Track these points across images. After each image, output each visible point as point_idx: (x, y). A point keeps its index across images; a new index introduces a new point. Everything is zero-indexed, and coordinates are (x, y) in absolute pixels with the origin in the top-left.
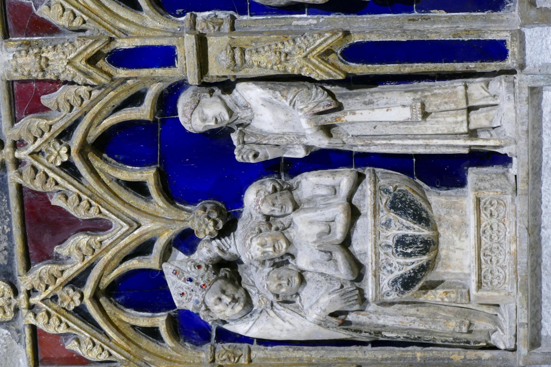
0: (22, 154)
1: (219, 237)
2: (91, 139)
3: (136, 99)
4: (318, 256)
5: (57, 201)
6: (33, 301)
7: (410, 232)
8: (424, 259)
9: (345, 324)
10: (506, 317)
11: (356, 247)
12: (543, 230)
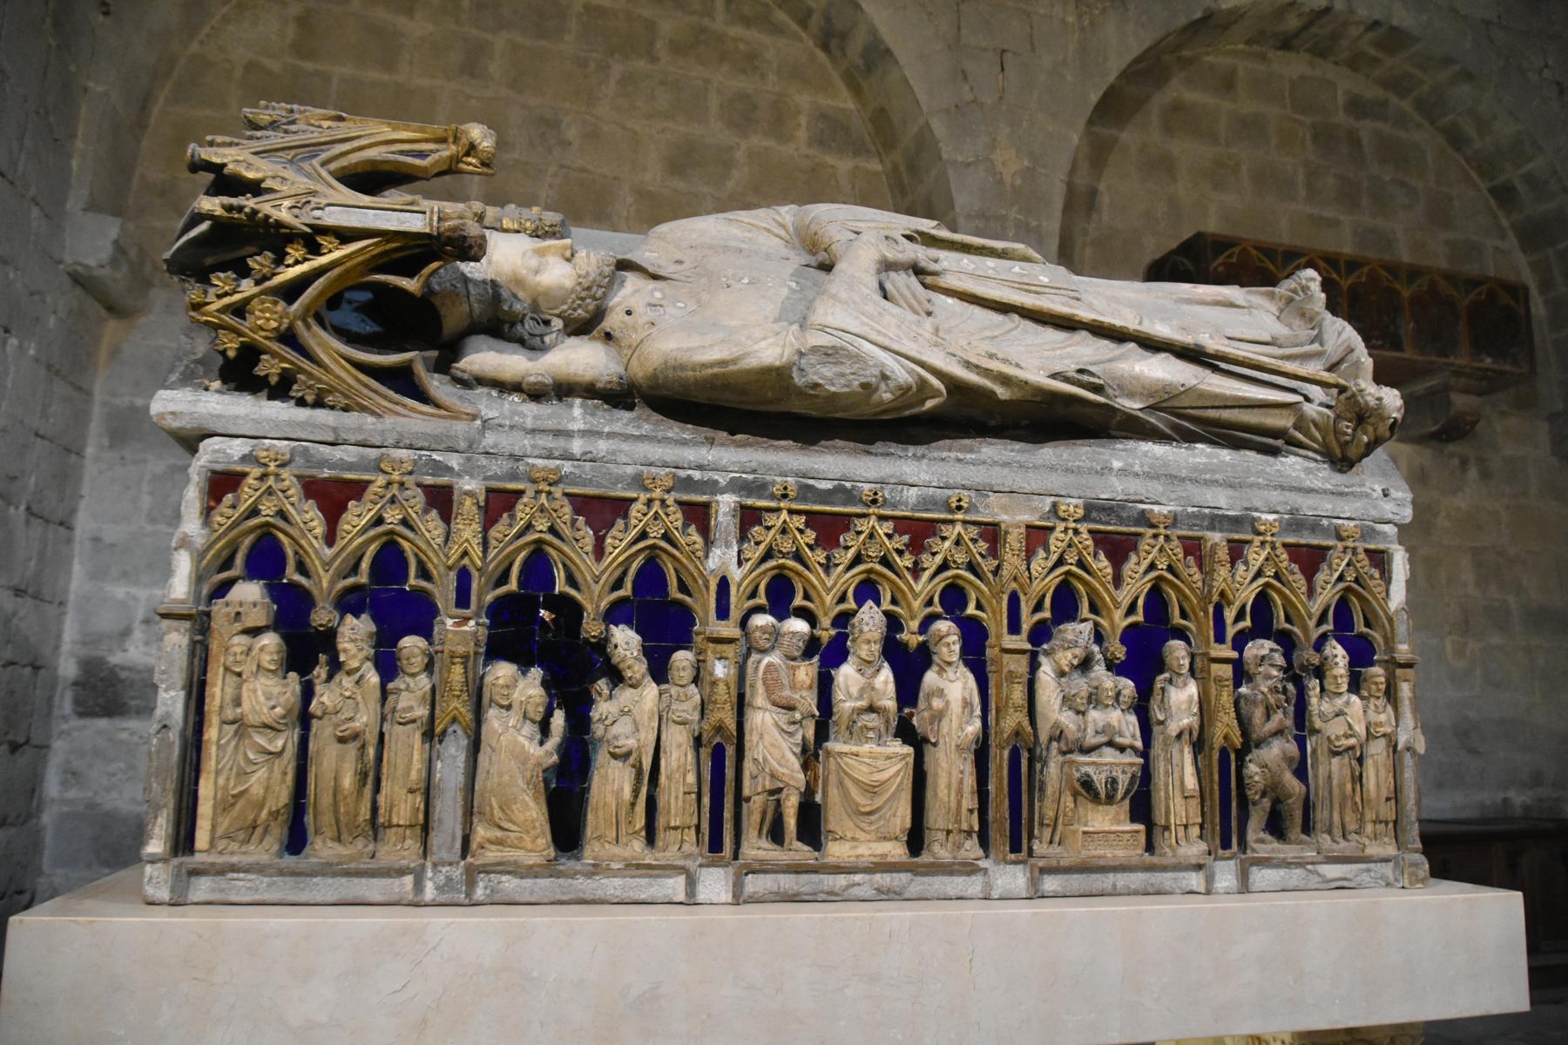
0: (1161, 538)
1: (1106, 659)
3: (1184, 615)
4: (1101, 724)
5: (1133, 558)
9: (1051, 739)
10: (1055, 850)
11: (1108, 750)
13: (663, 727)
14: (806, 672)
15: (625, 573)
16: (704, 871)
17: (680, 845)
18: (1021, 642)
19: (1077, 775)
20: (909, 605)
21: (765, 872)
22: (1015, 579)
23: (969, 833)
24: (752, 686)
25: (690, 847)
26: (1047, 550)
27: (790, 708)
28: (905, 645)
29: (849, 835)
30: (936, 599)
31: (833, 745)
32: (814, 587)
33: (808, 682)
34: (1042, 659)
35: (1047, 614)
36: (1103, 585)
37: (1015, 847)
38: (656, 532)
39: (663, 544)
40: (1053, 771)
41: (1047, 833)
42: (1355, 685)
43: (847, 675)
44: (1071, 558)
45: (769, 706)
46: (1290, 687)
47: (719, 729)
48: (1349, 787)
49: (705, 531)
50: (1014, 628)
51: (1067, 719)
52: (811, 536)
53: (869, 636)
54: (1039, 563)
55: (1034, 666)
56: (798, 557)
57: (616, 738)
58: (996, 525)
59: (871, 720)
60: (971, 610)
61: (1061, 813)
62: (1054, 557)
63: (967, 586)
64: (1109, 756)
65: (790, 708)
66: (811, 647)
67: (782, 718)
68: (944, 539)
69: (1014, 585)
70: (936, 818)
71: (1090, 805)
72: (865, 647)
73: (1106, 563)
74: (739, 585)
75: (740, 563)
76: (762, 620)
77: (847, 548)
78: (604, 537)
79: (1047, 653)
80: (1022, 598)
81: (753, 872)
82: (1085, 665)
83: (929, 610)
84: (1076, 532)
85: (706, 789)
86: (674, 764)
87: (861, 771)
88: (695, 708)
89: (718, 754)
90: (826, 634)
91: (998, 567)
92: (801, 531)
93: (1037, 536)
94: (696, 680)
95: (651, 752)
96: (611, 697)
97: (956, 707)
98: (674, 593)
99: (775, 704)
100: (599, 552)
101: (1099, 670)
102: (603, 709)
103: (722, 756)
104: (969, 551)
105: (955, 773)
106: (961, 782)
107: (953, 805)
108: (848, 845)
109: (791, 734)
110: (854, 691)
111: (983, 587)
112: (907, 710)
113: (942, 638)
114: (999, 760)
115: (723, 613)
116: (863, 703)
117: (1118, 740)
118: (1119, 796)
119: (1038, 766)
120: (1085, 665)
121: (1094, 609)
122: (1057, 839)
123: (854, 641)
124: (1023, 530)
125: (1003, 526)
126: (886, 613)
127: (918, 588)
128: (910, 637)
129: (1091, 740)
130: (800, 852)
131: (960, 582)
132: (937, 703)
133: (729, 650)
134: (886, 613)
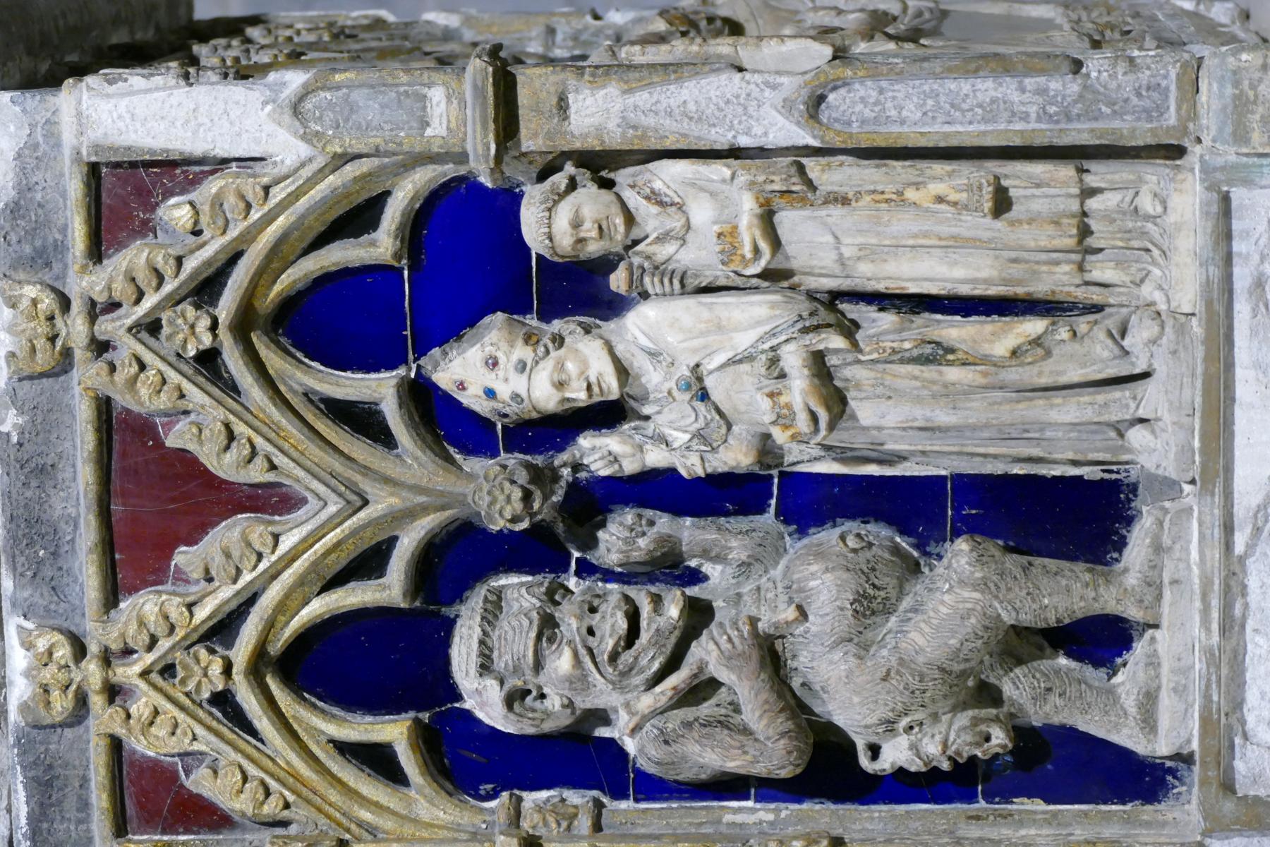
2: (276, 647)
42: (582, 290)
46: (619, 538)
48: (953, 374)
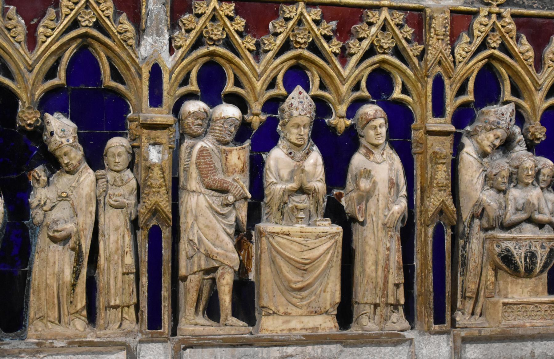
4: (521, 202)
6: (494, 16)
7: (539, 261)
8: (522, 269)
9: (473, 217)
10: (477, 320)
11: (528, 227)
12: (531, 343)
13: (101, 211)
14: (239, 156)
15: (58, 62)
16: (144, 346)
17: (121, 322)
18: (445, 124)
19: (498, 250)
20: (337, 90)
21: (202, 346)
22: (440, 63)
23: (395, 306)
24: (186, 171)
25: (130, 324)
26: (471, 35)
27: (224, 191)
28: (334, 128)
29: (282, 310)
30: (363, 84)
31: (265, 226)
32: (245, 74)
33: (240, 165)
34: (466, 140)
35: (470, 97)
36: (524, 67)
37: (439, 319)
38: (87, 20)
39: (95, 33)
40: (475, 246)
41: (469, 305)
43: (277, 158)
44: (494, 42)
45: (203, 190)
47: (155, 212)
49: (136, 19)
50: (438, 110)
51: (489, 198)
52: (240, 23)
53: (298, 120)
54: (463, 47)
55: (458, 147)
56: (228, 44)
57: (55, 222)
58: (421, 10)
59: (302, 201)
60: (397, 94)
61: (482, 286)
62: (478, 42)
63: (394, 71)
64: (529, 232)
65: (224, 191)
66: (243, 132)
67: (216, 200)
68: (370, 24)
69: (439, 69)
70: (364, 292)
71: (510, 279)
72: (295, 131)
73: (528, 46)
74: (171, 72)
75: (171, 51)
76: (194, 106)
77: (276, 35)
78: (36, 26)
79: (470, 135)
80: (447, 81)
81: (191, 347)
82: (506, 145)
83: (357, 94)
84: (499, 16)
85: (144, 269)
86: (113, 247)
87: (293, 251)
88: (131, 193)
89: (155, 236)
90: (257, 119)
91: (423, 52)
92: (231, 19)
93: (461, 20)
94: (131, 166)
95: (89, 234)
96: (48, 183)
97: (383, 188)
98: (108, 81)
99: (208, 187)
100: (32, 41)
101: (520, 151)
102: (40, 195)
103: (159, 237)
104: (394, 36)
105: (382, 250)
106: (388, 259)
107: (381, 281)
108: (281, 319)
109: (224, 216)
110: (285, 173)
111: (409, 71)
112: (335, 192)
113: (368, 122)
114: (424, 237)
115: (156, 99)
116: (294, 185)
117: (538, 216)
118: (538, 270)
119: (461, 242)
120: (506, 145)
121: (515, 91)
122: (478, 310)
123: (284, 125)
124: (448, 15)
125: (428, 12)
126: (315, 98)
127: (345, 73)
128: (338, 121)
129: (511, 217)
130: (236, 327)
131: (386, 67)
132: (364, 184)
133: (163, 136)
134: (315, 98)
